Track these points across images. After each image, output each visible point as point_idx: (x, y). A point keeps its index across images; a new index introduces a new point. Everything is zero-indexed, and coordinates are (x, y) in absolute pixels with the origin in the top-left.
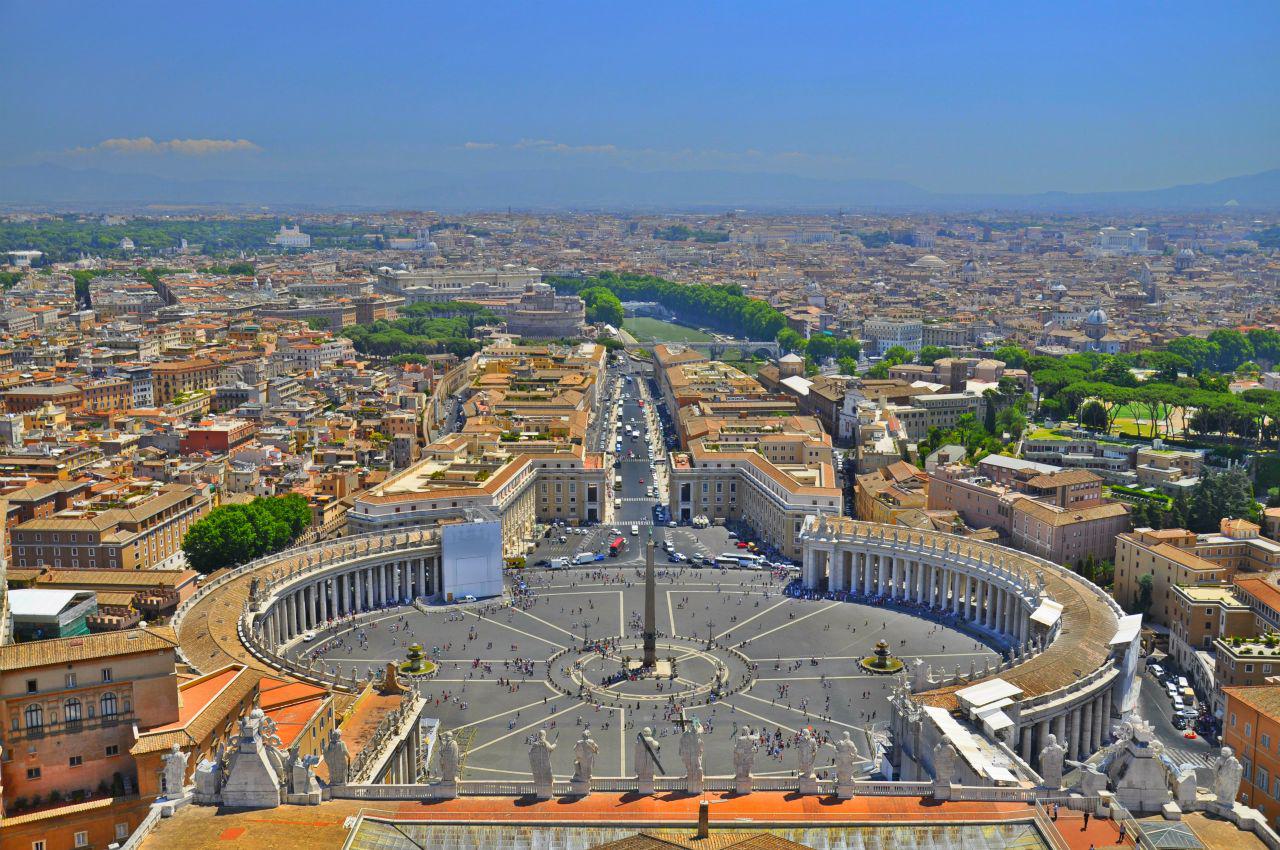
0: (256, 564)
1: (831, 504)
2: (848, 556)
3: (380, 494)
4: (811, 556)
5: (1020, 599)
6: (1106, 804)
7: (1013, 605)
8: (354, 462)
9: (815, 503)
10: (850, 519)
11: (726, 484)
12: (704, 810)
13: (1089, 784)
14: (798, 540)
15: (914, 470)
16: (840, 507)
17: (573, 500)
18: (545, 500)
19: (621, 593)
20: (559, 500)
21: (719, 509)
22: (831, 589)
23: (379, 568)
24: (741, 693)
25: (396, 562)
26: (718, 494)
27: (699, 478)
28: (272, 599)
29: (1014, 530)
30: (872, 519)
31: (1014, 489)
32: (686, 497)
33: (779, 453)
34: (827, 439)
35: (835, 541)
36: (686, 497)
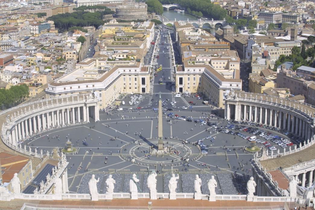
0: (9, 110)
1: (237, 85)
2: (243, 107)
3: (58, 82)
4: (228, 106)
5: (308, 123)
6: (312, 202)
7: (305, 126)
8: (50, 70)
9: (231, 85)
10: (244, 92)
11: (198, 77)
12: (150, 205)
13: (306, 196)
14: (224, 100)
15: (272, 72)
16: (240, 86)
17: (136, 84)
18: (125, 84)
19: (152, 121)
20: (130, 84)
21: (194, 87)
22: (236, 120)
23: (56, 111)
24: (196, 161)
25: (63, 109)
26: (195, 82)
27: (186, 74)
28: (14, 123)
29: (309, 96)
30: (254, 92)
31: (309, 80)
32: (181, 83)
33: (219, 65)
34: (238, 59)
35: (237, 99)
36: (181, 83)
